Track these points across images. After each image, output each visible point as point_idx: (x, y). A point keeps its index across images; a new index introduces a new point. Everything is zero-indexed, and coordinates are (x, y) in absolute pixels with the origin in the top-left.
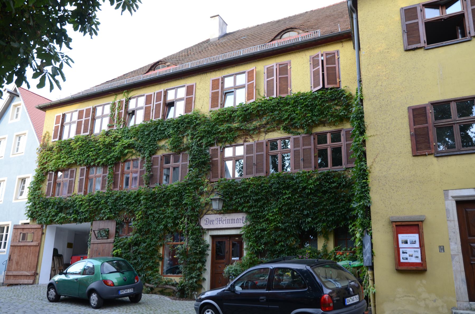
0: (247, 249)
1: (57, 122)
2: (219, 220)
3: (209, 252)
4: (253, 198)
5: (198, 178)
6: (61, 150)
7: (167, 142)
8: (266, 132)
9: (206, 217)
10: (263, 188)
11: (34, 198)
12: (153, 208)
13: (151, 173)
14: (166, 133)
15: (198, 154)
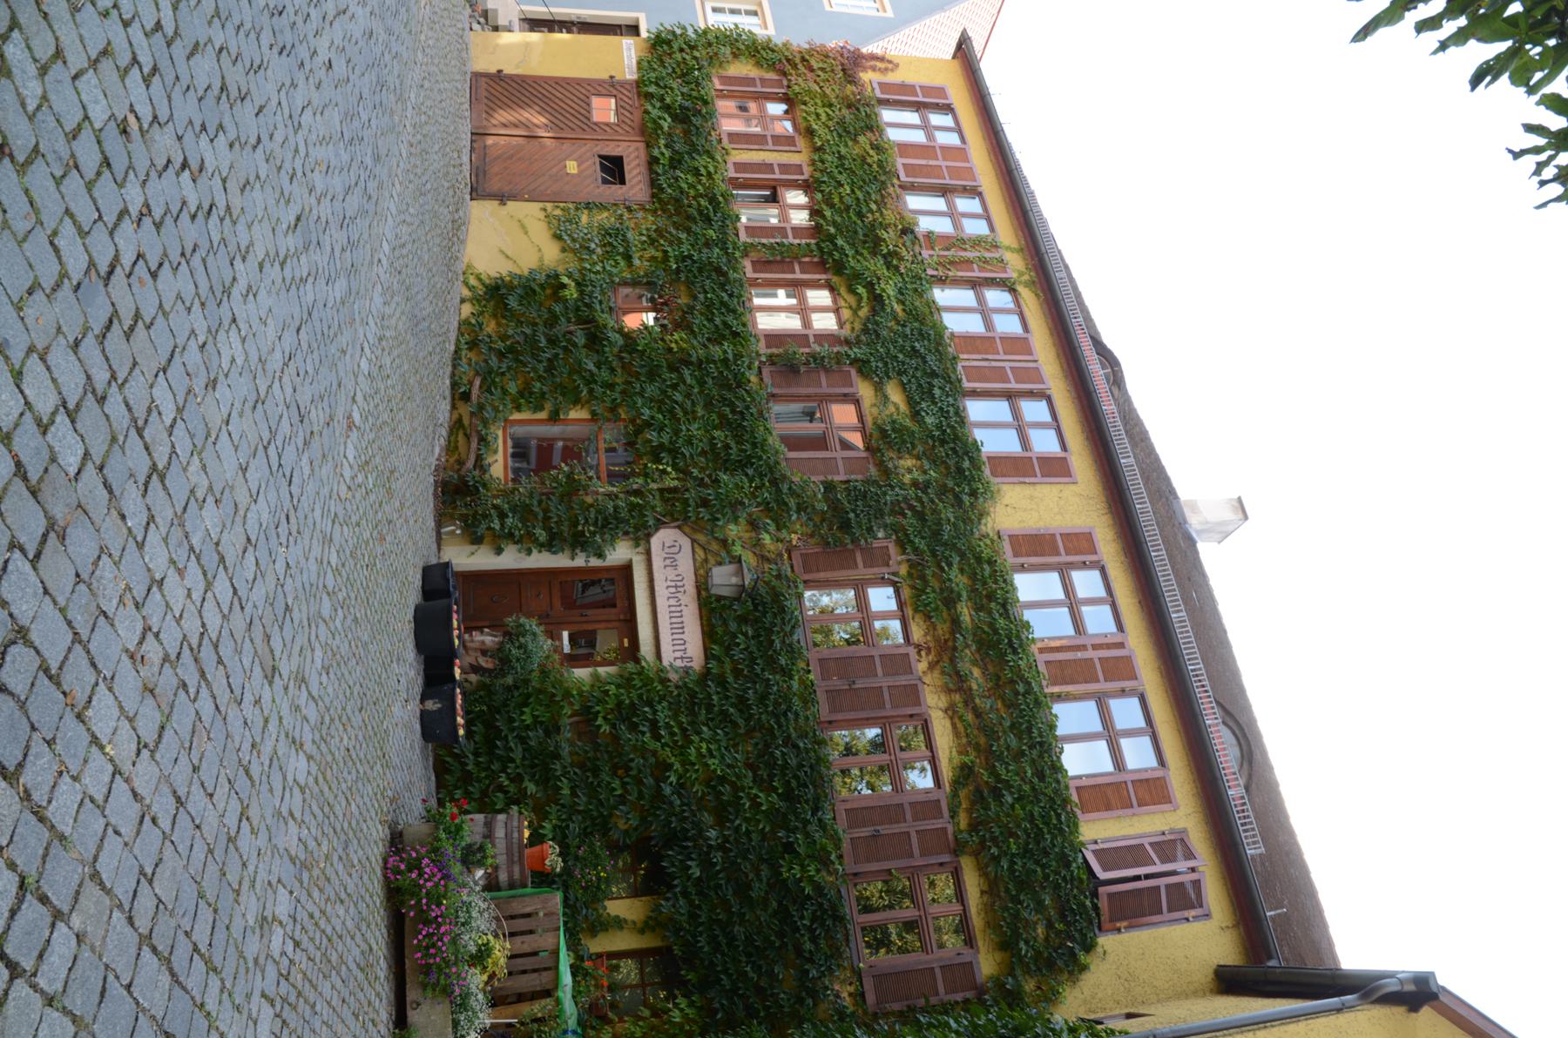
0: (596, 676)
1: (926, 90)
2: (679, 584)
3: (579, 561)
4: (749, 688)
5: (798, 512)
6: (849, 107)
7: (898, 409)
8: (951, 711)
9: (685, 543)
10: (783, 720)
11: (710, 44)
12: (702, 383)
13: (803, 369)
14: (924, 405)
15: (870, 507)
